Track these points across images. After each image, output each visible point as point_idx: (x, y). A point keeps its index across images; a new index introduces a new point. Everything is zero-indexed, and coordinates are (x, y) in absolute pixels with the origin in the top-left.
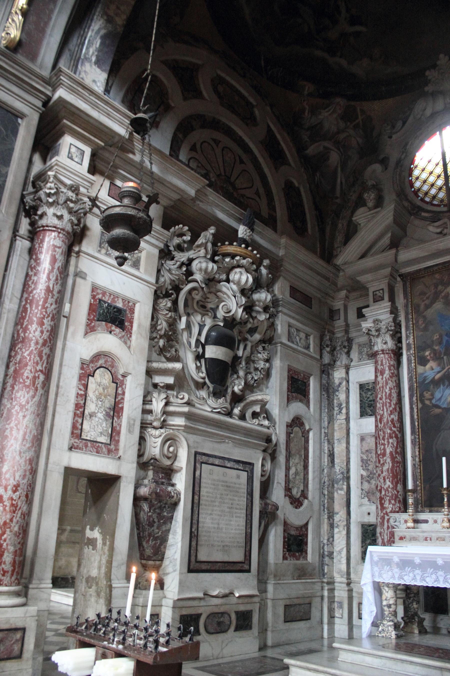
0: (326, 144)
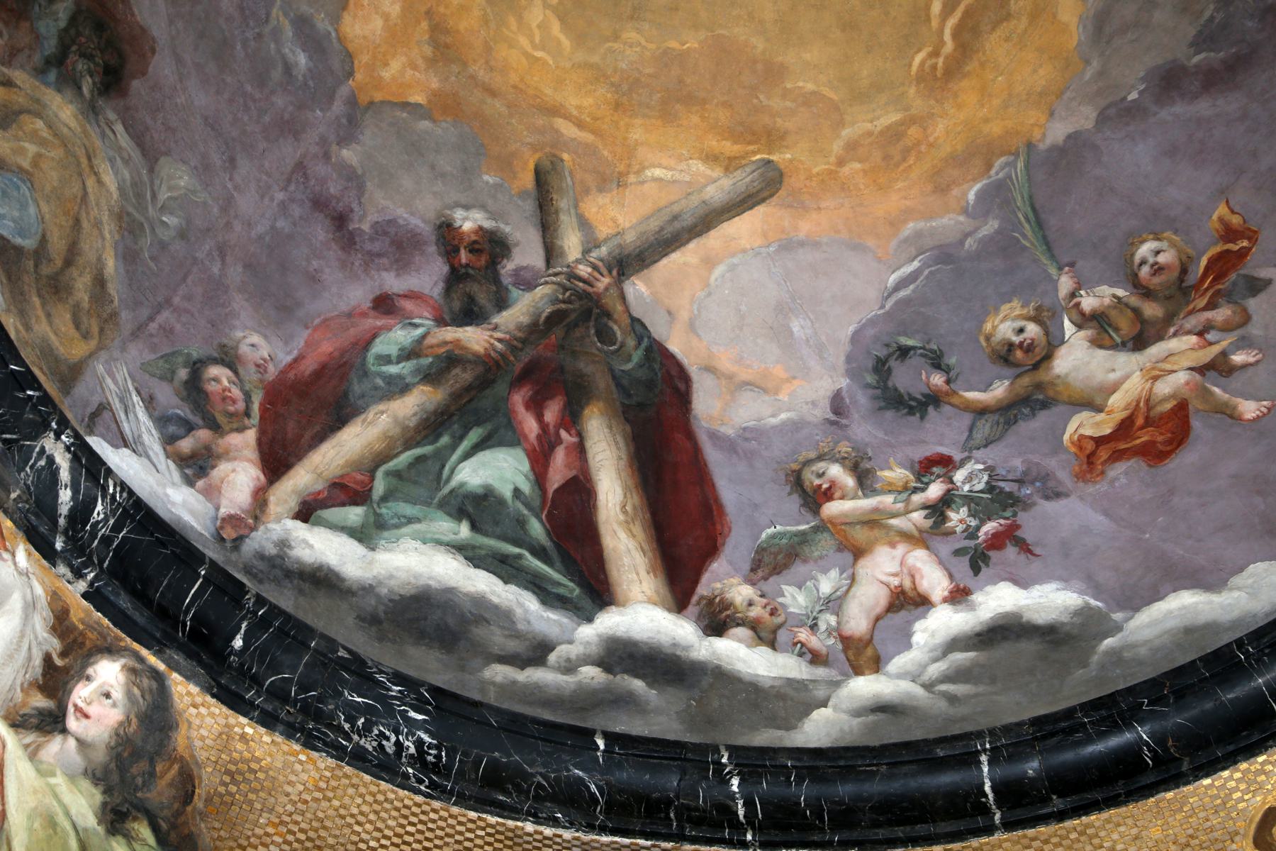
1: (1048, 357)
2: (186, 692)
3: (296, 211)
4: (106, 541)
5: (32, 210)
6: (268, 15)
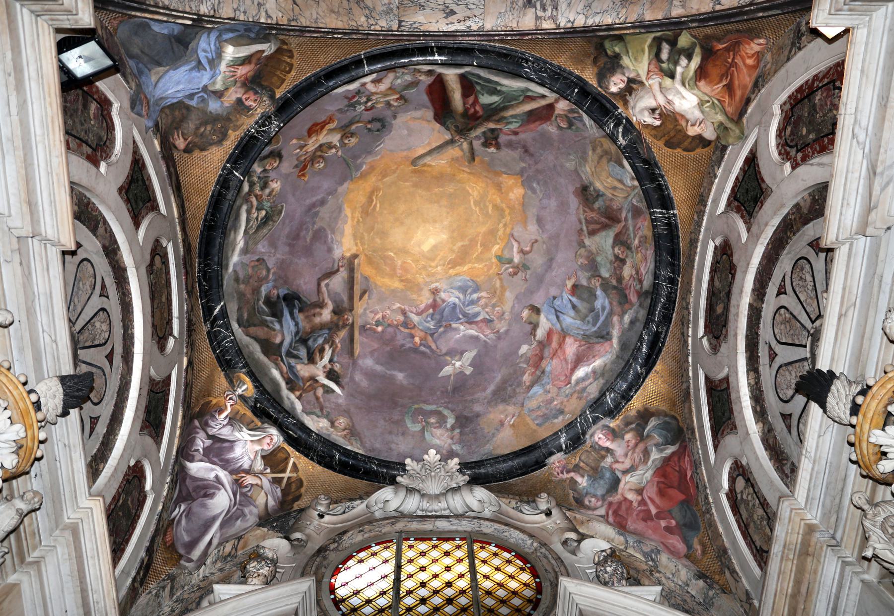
0: (223, 475)
1: (342, 137)
2: (593, 82)
4: (610, 118)
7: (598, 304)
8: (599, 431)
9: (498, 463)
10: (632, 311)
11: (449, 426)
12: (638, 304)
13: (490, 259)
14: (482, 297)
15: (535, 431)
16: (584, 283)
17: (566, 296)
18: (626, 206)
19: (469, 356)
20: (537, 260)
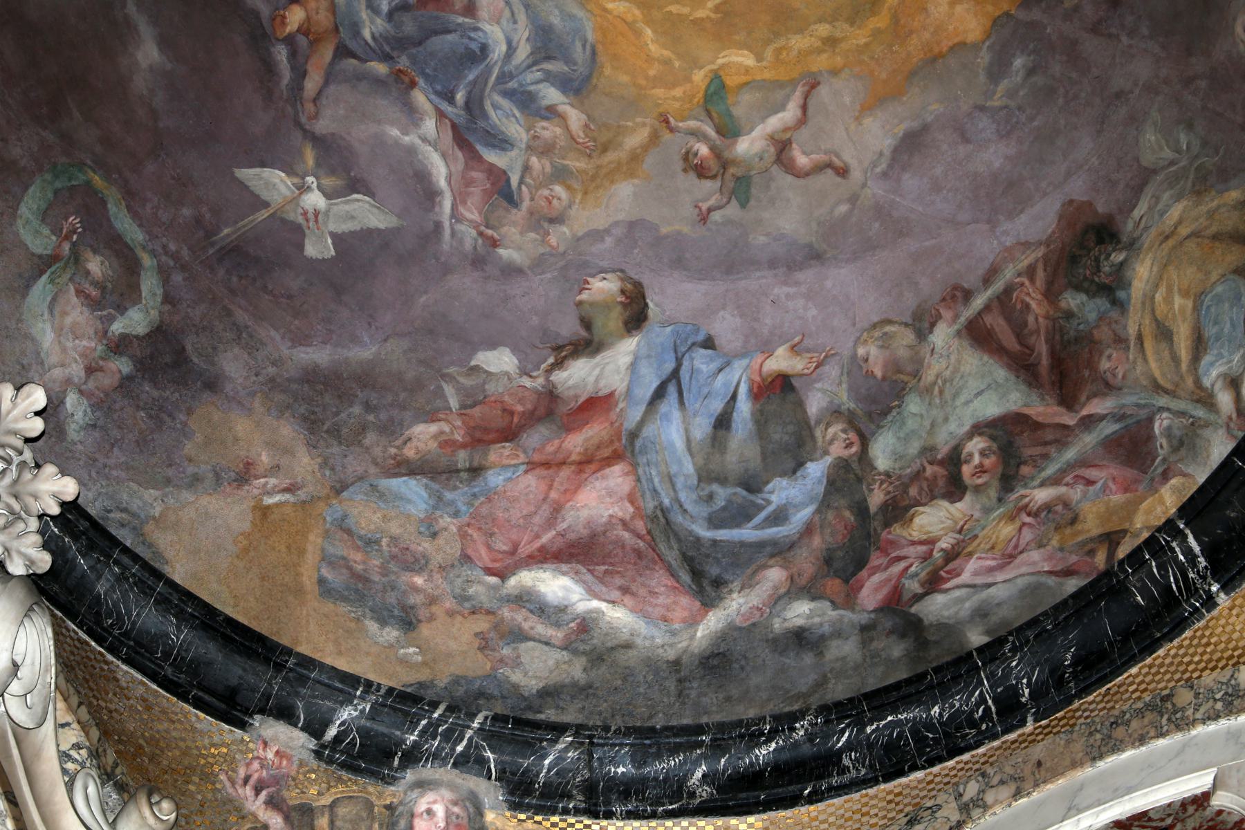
3: (1129, 20)
5: (1219, 289)
6: (1002, 108)
7: (781, 491)
8: (447, 794)
9: (146, 590)
10: (833, 614)
11: (117, 327)
12: (864, 618)
13: (696, 64)
14: (562, 117)
15: (299, 591)
16: (815, 404)
17: (739, 376)
18: (1129, 400)
19: (362, 213)
20: (787, 214)
